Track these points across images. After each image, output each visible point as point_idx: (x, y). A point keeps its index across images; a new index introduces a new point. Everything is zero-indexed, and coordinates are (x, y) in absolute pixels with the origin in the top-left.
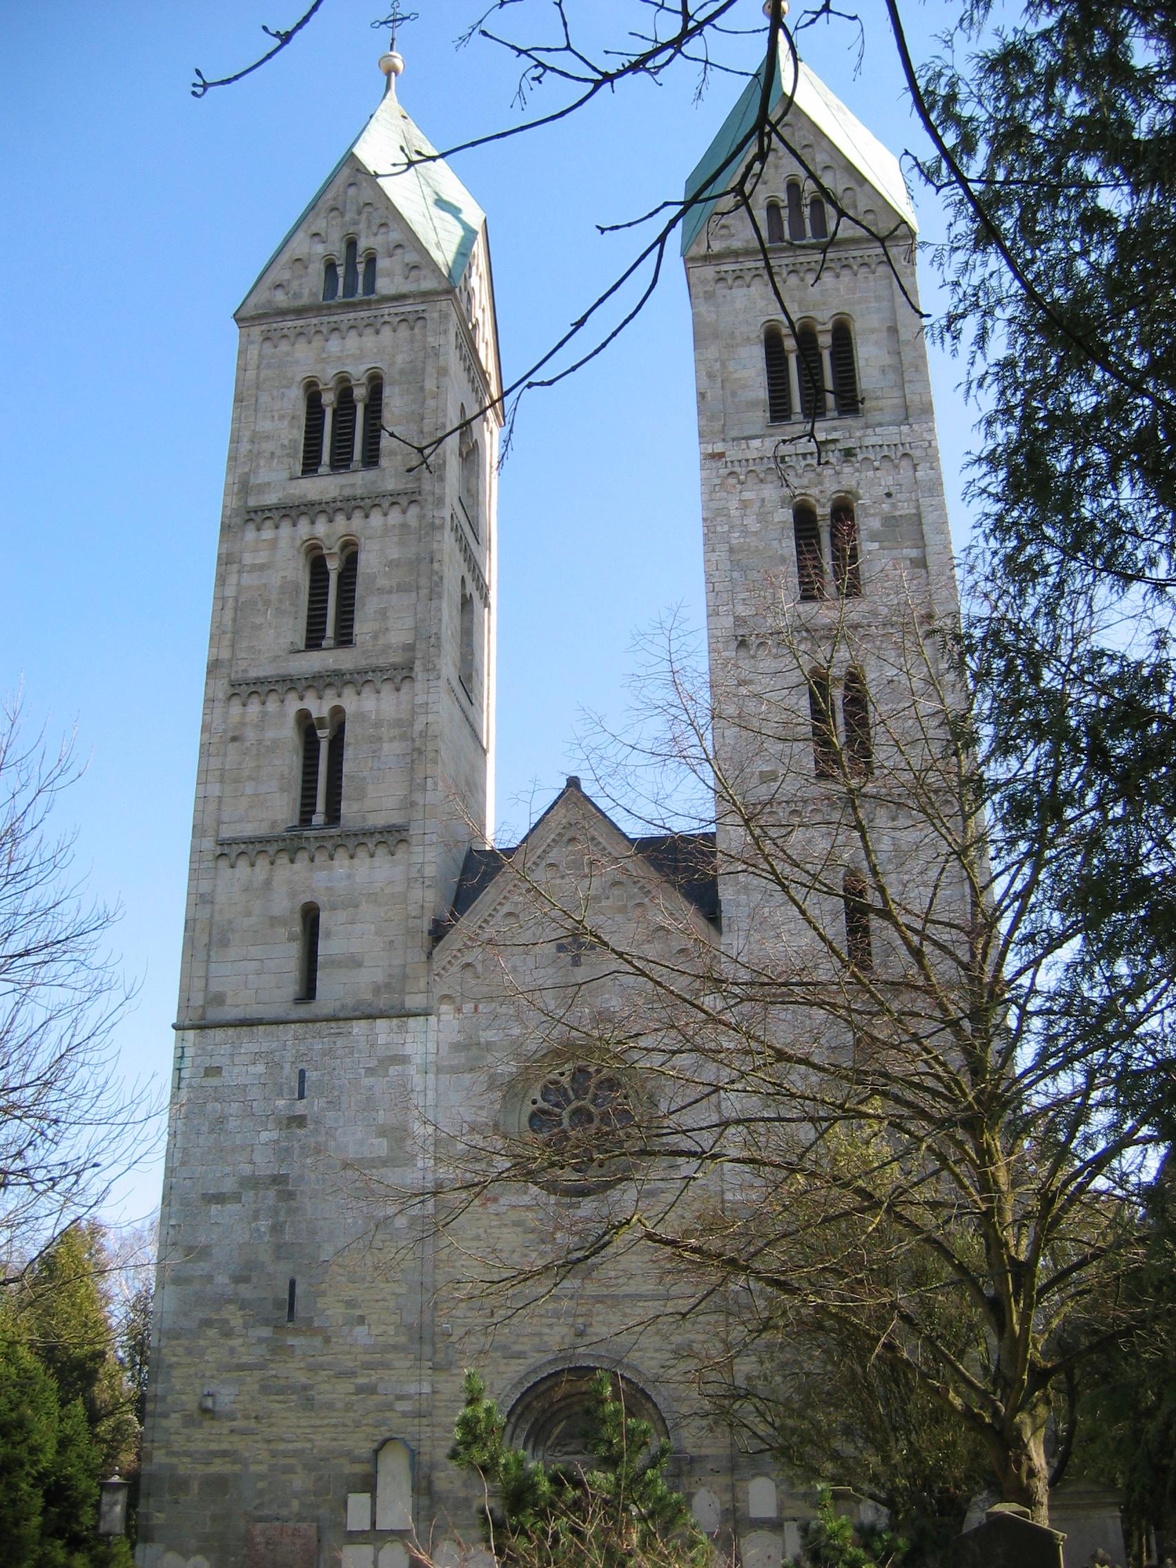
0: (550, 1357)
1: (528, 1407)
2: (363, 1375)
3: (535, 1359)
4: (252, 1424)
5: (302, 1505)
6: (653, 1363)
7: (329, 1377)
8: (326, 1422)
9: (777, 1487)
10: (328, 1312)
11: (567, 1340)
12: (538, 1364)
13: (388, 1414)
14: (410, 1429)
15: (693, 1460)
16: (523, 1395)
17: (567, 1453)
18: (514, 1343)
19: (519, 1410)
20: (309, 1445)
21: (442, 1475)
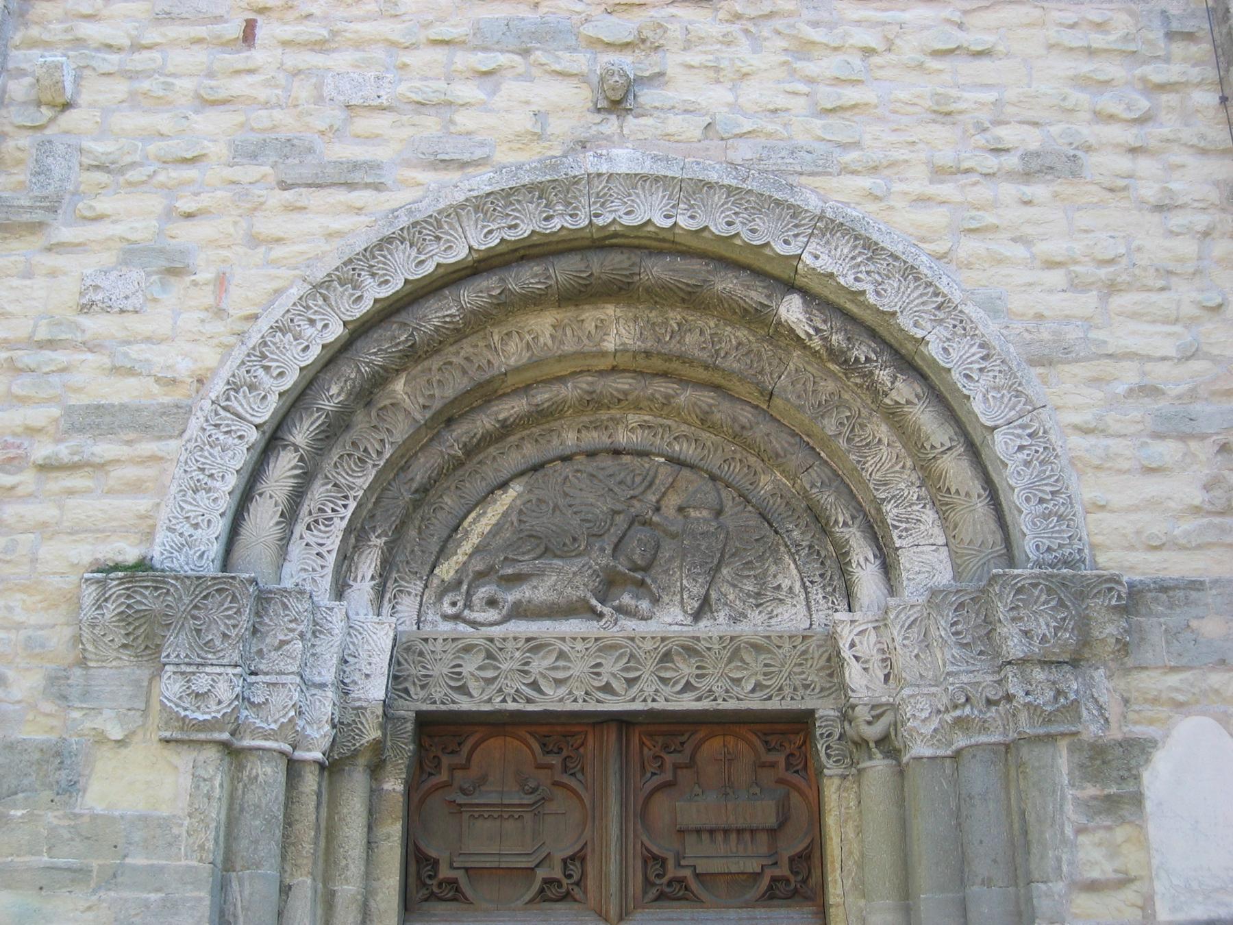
0: (482, 182)
1: (368, 393)
3: (418, 191)
6: (934, 217)
11: (560, 127)
12: (427, 208)
15: (1133, 600)
16: (359, 331)
17: (519, 612)
18: (332, 133)
19: (333, 395)
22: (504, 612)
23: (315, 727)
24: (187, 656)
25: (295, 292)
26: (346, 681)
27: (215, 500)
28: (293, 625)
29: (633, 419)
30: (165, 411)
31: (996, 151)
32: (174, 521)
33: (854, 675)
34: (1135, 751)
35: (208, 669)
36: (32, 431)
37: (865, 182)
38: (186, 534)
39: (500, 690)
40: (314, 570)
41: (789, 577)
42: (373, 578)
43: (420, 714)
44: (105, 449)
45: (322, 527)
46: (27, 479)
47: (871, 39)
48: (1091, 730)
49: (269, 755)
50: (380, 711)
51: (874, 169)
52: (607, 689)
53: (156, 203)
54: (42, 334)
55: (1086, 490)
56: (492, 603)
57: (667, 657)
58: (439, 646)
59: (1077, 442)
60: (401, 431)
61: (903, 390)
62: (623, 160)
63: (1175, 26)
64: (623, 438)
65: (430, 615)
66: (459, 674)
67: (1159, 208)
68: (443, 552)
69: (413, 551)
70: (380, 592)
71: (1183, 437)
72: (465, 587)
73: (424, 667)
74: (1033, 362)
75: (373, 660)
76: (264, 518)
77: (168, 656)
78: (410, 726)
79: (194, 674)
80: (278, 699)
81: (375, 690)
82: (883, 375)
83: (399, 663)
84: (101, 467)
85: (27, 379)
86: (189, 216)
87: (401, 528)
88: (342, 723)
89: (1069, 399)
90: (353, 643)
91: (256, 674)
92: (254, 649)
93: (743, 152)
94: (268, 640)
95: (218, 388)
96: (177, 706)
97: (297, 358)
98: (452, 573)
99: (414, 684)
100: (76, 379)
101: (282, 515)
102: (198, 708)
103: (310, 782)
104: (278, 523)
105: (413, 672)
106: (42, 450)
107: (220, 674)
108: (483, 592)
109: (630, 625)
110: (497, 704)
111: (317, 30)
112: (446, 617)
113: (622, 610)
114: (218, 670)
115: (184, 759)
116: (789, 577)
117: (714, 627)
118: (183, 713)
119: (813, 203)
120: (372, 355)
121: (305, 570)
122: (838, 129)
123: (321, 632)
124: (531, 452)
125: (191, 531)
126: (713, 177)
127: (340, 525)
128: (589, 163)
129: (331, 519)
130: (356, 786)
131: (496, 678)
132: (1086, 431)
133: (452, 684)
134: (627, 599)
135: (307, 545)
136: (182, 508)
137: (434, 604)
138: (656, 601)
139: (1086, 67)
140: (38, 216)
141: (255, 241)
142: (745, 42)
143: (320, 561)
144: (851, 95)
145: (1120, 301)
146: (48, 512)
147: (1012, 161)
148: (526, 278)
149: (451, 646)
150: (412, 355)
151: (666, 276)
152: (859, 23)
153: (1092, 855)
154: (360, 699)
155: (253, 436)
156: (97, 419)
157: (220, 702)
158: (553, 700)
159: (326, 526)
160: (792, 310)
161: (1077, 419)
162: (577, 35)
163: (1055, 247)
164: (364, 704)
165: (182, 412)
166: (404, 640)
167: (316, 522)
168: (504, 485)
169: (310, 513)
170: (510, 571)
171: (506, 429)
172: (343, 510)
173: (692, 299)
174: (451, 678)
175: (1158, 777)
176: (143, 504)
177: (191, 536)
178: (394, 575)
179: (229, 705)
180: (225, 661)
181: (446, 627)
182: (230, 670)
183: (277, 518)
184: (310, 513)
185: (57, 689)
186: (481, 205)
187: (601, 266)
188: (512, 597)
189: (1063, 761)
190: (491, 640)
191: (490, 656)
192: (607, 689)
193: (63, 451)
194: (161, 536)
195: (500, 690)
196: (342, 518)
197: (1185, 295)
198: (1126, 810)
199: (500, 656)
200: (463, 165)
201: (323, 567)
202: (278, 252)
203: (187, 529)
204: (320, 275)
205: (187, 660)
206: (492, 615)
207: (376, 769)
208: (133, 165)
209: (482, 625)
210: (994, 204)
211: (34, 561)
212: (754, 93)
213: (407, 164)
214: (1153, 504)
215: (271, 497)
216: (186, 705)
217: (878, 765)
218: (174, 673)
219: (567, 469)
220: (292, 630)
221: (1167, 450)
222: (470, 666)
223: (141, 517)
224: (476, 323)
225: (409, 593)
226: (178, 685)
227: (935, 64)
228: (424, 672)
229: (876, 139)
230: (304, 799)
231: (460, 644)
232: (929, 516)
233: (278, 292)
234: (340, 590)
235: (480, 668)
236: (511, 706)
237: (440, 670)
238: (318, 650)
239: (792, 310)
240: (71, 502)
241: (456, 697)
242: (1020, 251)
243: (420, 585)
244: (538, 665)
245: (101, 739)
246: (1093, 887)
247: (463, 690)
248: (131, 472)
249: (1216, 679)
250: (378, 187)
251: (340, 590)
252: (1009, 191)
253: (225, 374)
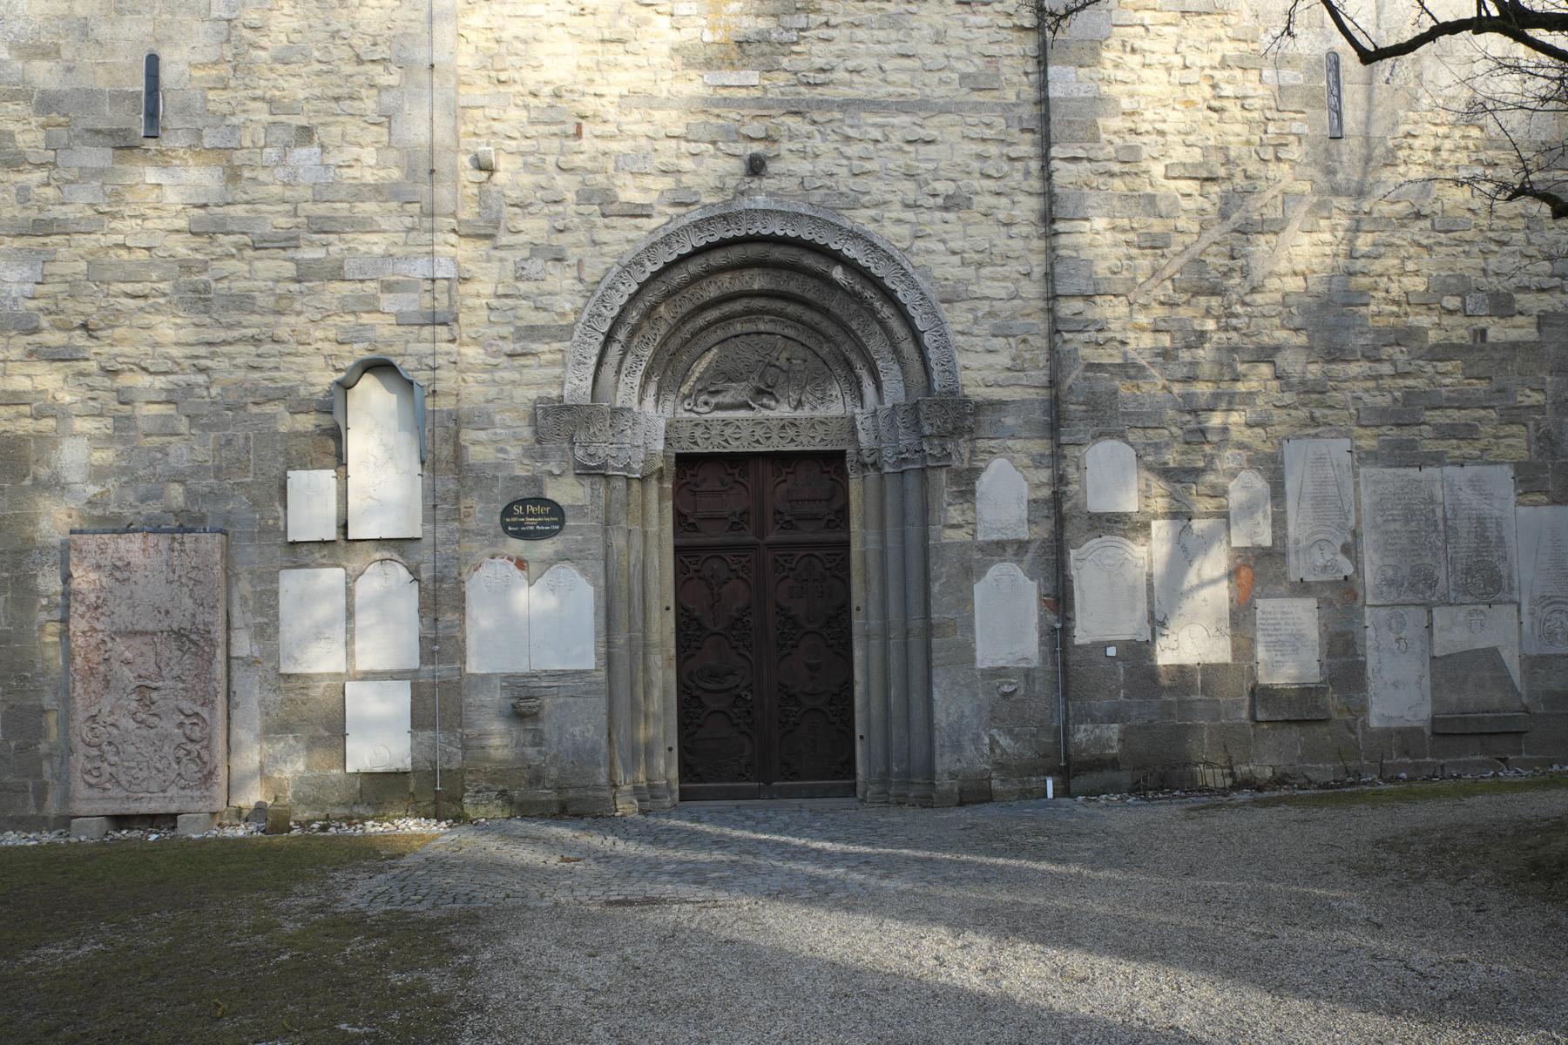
0: (696, 214)
1: (649, 314)
2: (311, 243)
4: (79, 339)
5: (191, 495)
6: (904, 230)
7: (241, 248)
8: (236, 334)
9: (1139, 457)
10: (234, 120)
11: (731, 182)
12: (672, 227)
13: (366, 319)
14: (414, 347)
16: (643, 286)
17: (719, 407)
19: (634, 317)
20: (201, 379)
21: (482, 435)
25: (616, 269)
29: (767, 318)
30: (562, 328)
31: (934, 196)
33: (862, 436)
34: (975, 472)
36: (503, 338)
37: (873, 212)
41: (836, 391)
44: (535, 347)
46: (503, 360)
47: (878, 135)
48: (956, 464)
51: (876, 205)
52: (758, 441)
53: (544, 224)
54: (501, 291)
55: (961, 360)
56: (706, 403)
57: (783, 427)
59: (960, 338)
60: (663, 329)
61: (886, 312)
62: (761, 201)
63: (1025, 125)
64: (762, 327)
65: (680, 410)
67: (1005, 225)
68: (683, 382)
70: (657, 402)
71: (1006, 336)
74: (943, 301)
76: (608, 372)
81: (659, 446)
82: (878, 305)
85: (496, 313)
86: (561, 231)
87: (666, 371)
89: (957, 318)
93: (816, 197)
95: (585, 316)
97: (619, 300)
100: (520, 312)
103: (636, 486)
106: (508, 347)
109: (766, 412)
110: (710, 449)
111: (610, 128)
113: (763, 406)
115: (587, 482)
116: (836, 391)
117: (804, 413)
119: (847, 224)
120: (649, 298)
122: (859, 184)
124: (721, 334)
126: (802, 211)
128: (746, 203)
130: (654, 483)
132: (962, 333)
134: (765, 401)
138: (777, 401)
139: (978, 148)
140: (489, 231)
141: (594, 243)
142: (818, 135)
144: (868, 166)
145: (985, 271)
146: (515, 376)
147: (940, 201)
148: (718, 258)
150: (669, 295)
151: (782, 257)
152: (874, 125)
153: (954, 514)
155: (602, 338)
156: (532, 333)
158: (734, 447)
160: (838, 273)
161: (959, 328)
162: (738, 133)
163: (956, 245)
165: (570, 329)
168: (709, 350)
171: (709, 325)
173: (794, 268)
175: (983, 484)
181: (686, 415)
185: (528, 453)
186: (696, 225)
187: (754, 251)
188: (713, 401)
189: (943, 476)
192: (758, 441)
193: (518, 347)
194: (567, 386)
197: (1014, 268)
198: (968, 497)
200: (687, 205)
202: (606, 249)
204: (625, 261)
206: (706, 409)
207: (660, 479)
208: (531, 204)
210: (932, 223)
211: (512, 398)
212: (821, 165)
213: (660, 203)
214: (991, 366)
217: (872, 474)
219: (737, 341)
221: (999, 342)
222: (698, 432)
224: (695, 280)
227: (907, 148)
229: (877, 187)
232: (896, 367)
233: (608, 270)
234: (641, 401)
239: (838, 273)
240: (525, 371)
242: (941, 247)
244: (728, 431)
245: (551, 474)
246: (953, 526)
247: (695, 443)
248: (549, 357)
249: (1010, 443)
250: (648, 216)
251: (641, 401)
252: (938, 215)
253: (587, 311)
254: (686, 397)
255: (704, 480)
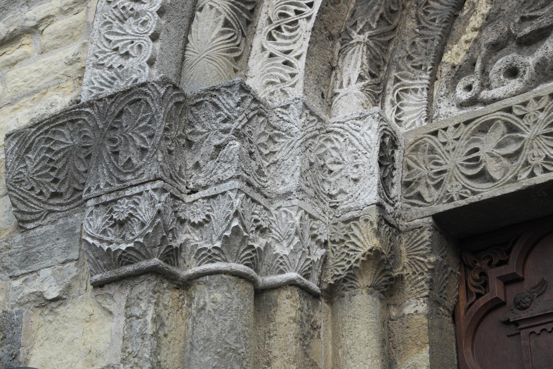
22: (526, 77)
23: (285, 243)
24: (108, 184)
26: (334, 192)
27: (144, 23)
28: (228, 125)
32: (101, 56)
35: (128, 193)
38: (115, 66)
39: (527, 164)
40: (283, 81)
42: (361, 78)
43: (437, 217)
45: (286, 34)
49: (217, 277)
50: (374, 216)
56: (512, 72)
58: (450, 135)
66: (477, 159)
68: (447, 37)
69: (414, 43)
72: (478, 66)
73: (437, 164)
75: (359, 161)
77: (89, 190)
78: (426, 235)
79: (115, 201)
80: (220, 210)
83: (409, 168)
84: (33, 30)
88: (334, 242)
90: (335, 148)
91: (193, 192)
92: (190, 165)
94: (202, 150)
96: (101, 240)
98: (463, 55)
99: (428, 186)
101: (226, 23)
102: (124, 238)
103: (288, 306)
104: (223, 33)
105: (425, 172)
107: (141, 194)
108: (501, 62)
110: (524, 181)
112: (462, 105)
114: (137, 190)
115: (118, 298)
118: (105, 247)
121: (272, 83)
123: (279, 136)
125: (122, 61)
127: (306, 27)
129: (296, 22)
130: (362, 310)
131: (518, 153)
133: (470, 172)
135: (271, 55)
136: (109, 41)
137: (447, 95)
143: (288, 70)
149: (463, 129)
154: (350, 210)
157: (143, 225)
159: (291, 31)
164: (355, 214)
166: (411, 140)
167: (279, 29)
169: (270, 21)
170: (527, 30)
172: (307, 10)
174: (468, 167)
176: (70, 51)
177: (121, 67)
178: (394, 74)
179: (151, 225)
180: (144, 178)
182: (149, 187)
183: (219, 28)
184: (270, 21)
190: (509, 110)
191: (511, 128)
195: (527, 164)
196: (308, 18)
199: (521, 124)
201: (292, 75)
203: (116, 61)
205: (108, 189)
206: (514, 84)
207: (389, 289)
209: (500, 99)
215: (211, 7)
216: (110, 238)
218: (97, 206)
220: (226, 131)
223: (71, 63)
225: (416, 91)
226: (100, 219)
228: (437, 169)
230: (281, 330)
231: (473, 126)
235: (499, 146)
236: (541, 178)
237: (452, 162)
238: (278, 156)
241: (475, 185)
243: (426, 76)
245: (45, 303)
247: (483, 176)
254: (459, 72)
255: (542, 287)
